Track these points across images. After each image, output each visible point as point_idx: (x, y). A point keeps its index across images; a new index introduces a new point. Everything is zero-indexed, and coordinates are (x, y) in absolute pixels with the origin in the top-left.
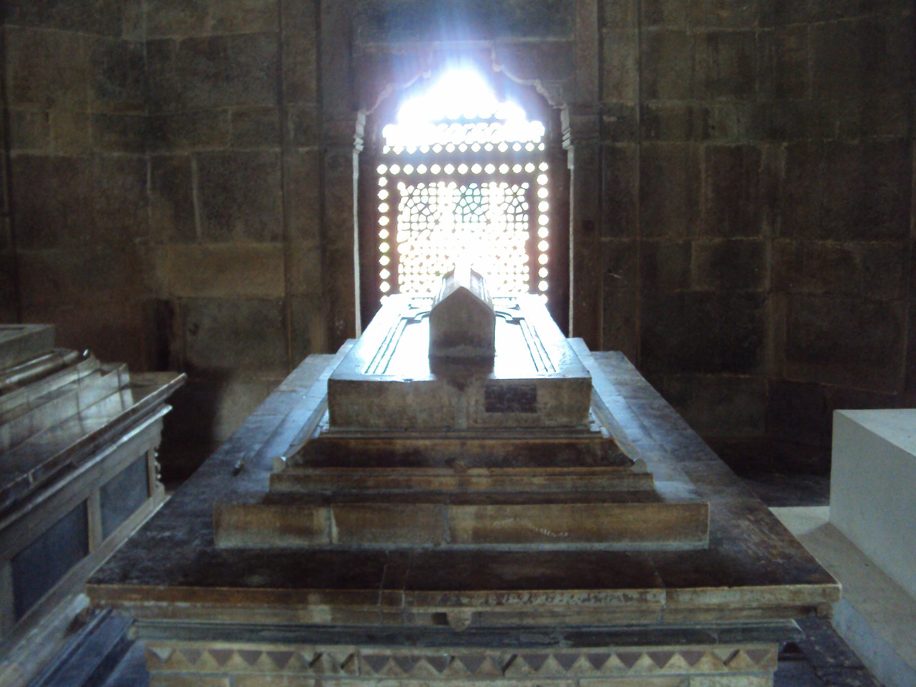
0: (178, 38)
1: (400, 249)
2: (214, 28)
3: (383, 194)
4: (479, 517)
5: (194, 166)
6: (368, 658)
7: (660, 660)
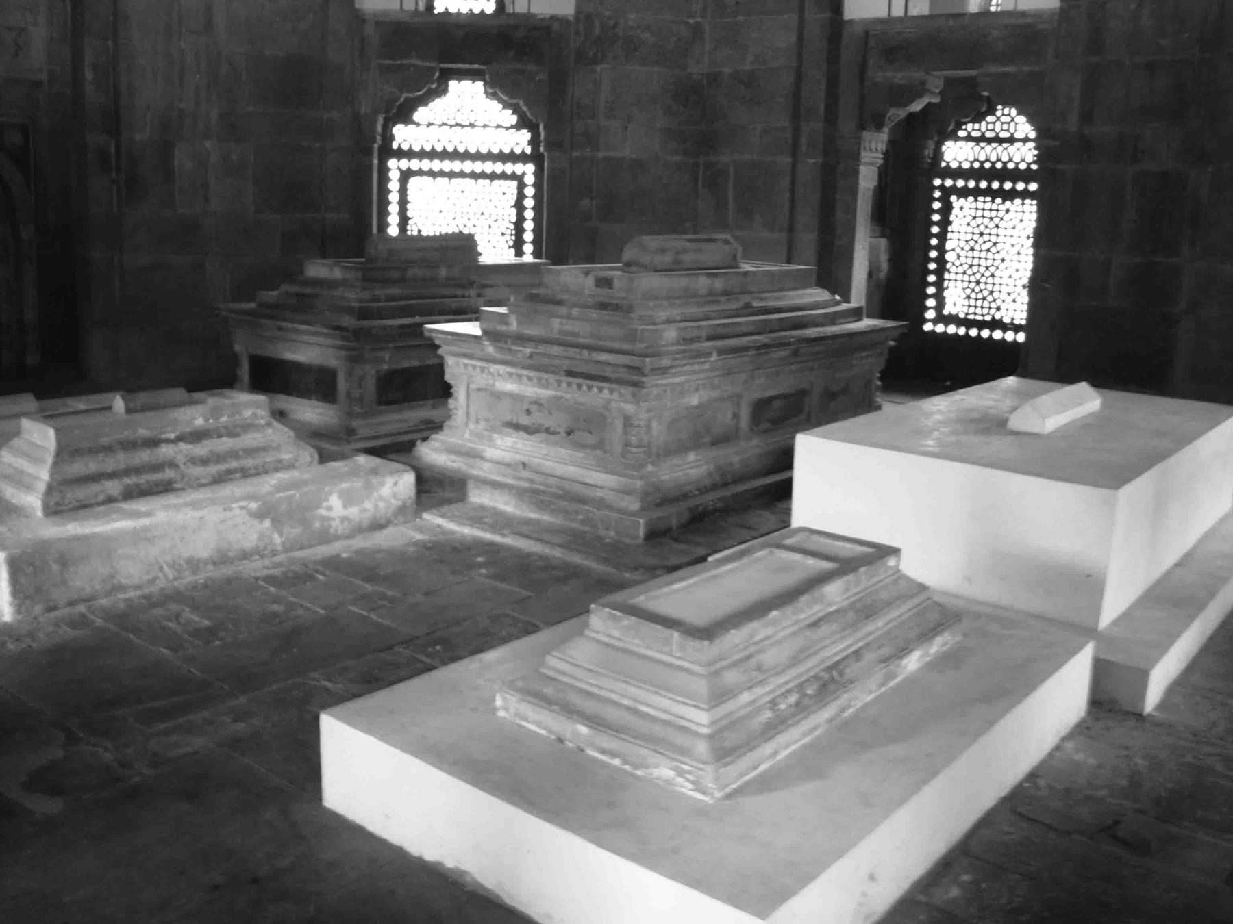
0: (727, 70)
1: (949, 256)
2: (752, 63)
3: (937, 205)
4: (561, 324)
5: (731, 169)
6: (508, 372)
7: (601, 390)
